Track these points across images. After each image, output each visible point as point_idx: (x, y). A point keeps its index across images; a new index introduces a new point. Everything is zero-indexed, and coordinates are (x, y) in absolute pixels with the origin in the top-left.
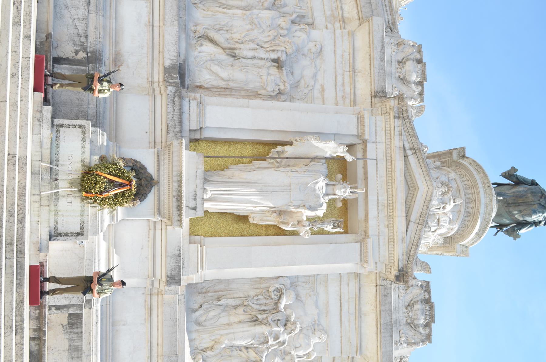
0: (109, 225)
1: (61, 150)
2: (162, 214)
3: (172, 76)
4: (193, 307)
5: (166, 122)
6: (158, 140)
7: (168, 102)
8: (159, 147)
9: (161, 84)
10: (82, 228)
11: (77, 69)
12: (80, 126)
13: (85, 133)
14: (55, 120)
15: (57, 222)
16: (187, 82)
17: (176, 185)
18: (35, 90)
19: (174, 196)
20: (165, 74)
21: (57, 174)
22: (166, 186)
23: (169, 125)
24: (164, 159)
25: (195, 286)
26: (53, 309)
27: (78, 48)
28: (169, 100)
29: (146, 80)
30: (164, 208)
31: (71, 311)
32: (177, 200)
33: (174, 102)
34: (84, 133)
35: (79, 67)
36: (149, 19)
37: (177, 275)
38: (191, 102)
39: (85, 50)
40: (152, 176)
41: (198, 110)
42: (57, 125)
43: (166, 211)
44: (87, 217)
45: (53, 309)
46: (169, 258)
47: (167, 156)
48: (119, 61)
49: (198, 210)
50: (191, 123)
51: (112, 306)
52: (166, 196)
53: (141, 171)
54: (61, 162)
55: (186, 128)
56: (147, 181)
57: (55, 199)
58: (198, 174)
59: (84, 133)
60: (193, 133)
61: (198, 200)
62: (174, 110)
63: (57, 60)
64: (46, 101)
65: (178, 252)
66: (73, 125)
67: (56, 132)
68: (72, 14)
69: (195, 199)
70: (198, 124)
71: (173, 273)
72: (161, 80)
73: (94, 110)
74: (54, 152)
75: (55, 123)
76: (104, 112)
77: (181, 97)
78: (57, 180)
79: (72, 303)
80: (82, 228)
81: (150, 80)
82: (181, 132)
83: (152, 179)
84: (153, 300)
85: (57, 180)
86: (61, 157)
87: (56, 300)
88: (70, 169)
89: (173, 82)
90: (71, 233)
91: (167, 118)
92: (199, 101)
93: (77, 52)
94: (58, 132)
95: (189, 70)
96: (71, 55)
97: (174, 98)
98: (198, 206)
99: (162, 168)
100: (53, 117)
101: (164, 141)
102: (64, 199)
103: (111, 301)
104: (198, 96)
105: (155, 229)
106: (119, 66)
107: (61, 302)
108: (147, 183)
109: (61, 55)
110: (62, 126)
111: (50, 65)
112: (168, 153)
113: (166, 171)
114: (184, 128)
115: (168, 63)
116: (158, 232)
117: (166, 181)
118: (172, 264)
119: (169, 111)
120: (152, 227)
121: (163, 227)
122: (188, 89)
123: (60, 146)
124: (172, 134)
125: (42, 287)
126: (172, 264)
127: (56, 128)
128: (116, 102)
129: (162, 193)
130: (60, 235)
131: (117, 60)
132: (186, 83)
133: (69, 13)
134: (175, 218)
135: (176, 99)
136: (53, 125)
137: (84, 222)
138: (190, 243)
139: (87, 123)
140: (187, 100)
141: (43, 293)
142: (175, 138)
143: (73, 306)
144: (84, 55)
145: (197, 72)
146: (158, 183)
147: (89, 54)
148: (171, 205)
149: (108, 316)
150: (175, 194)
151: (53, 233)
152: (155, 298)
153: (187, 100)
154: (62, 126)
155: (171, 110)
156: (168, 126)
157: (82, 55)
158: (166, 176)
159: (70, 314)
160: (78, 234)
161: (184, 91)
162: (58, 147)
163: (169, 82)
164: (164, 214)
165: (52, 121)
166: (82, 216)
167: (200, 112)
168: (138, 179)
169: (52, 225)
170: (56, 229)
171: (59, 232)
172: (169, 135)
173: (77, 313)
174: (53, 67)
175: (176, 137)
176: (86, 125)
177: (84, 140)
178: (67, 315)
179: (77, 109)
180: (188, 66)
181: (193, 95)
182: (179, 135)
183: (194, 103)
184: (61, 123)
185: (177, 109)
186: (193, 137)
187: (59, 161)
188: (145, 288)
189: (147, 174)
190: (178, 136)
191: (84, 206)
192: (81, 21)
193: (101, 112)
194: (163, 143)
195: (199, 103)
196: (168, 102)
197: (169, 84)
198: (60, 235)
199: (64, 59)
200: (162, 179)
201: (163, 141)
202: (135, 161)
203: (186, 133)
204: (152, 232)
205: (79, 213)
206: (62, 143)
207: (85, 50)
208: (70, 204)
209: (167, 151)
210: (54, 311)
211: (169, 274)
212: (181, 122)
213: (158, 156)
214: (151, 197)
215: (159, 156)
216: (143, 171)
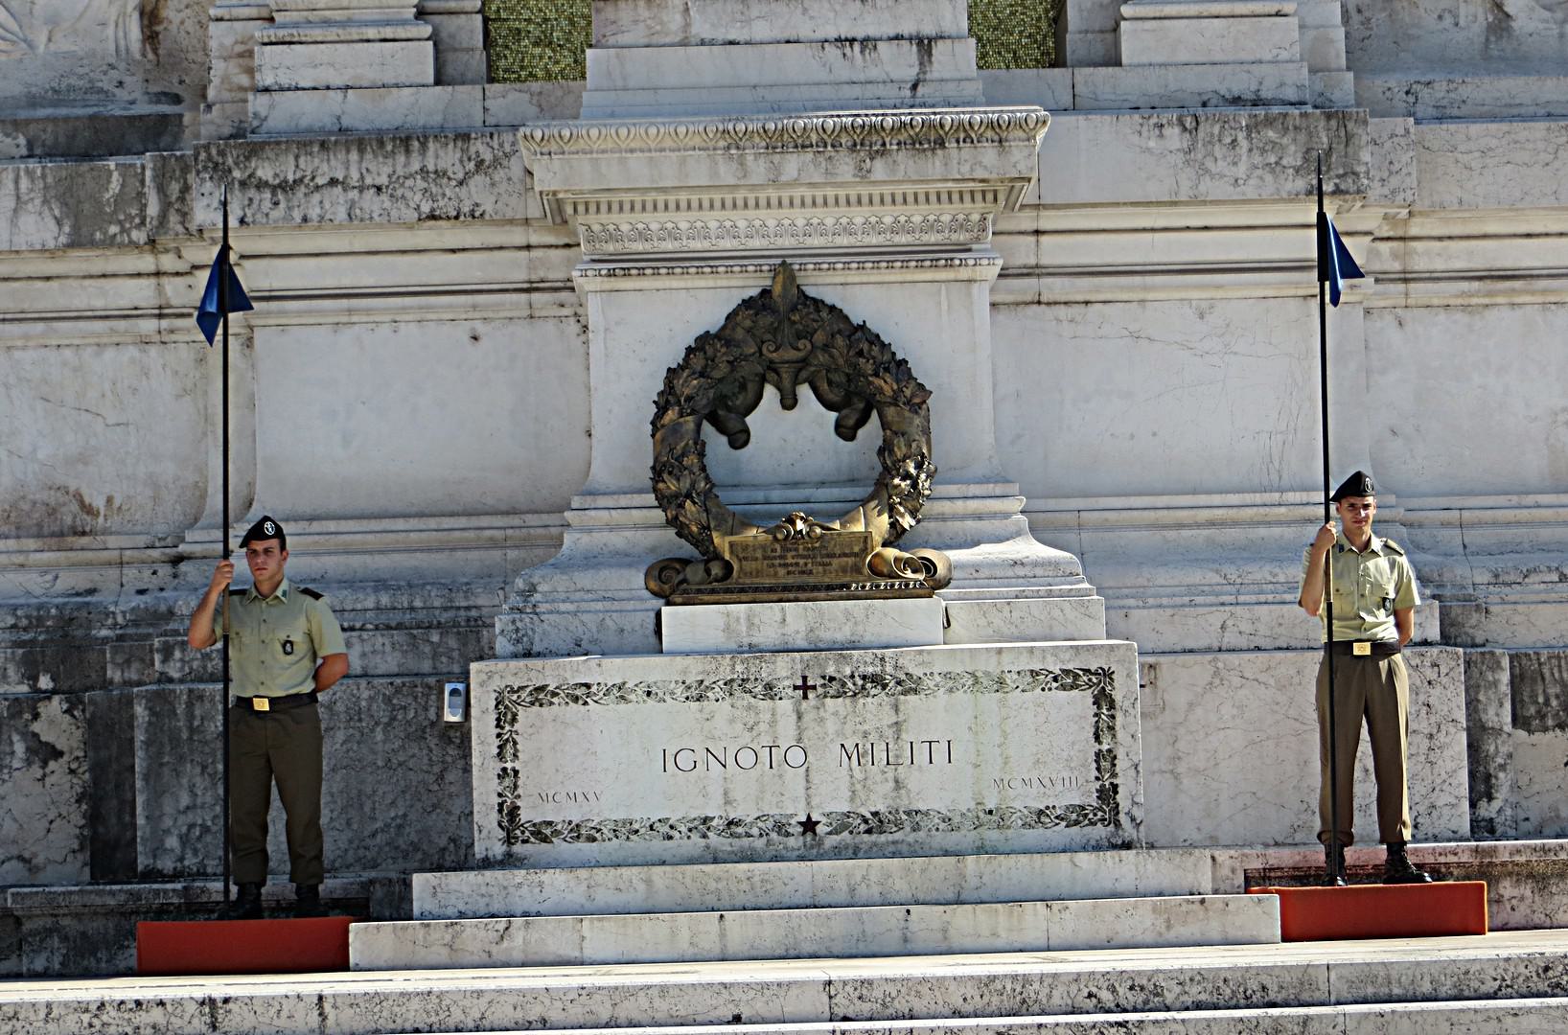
0: (1038, 532)
1: (642, 813)
2: (962, 237)
3: (119, 200)
4: (1478, 29)
5: (410, 227)
6: (514, 268)
7: (288, 217)
8: (553, 265)
9: (168, 262)
10: (1068, 680)
11: (148, 744)
12: (505, 717)
13: (541, 689)
14: (479, 851)
15: (1041, 813)
16: (134, 100)
17: (792, 164)
18: (339, 962)
19: (863, 174)
20: (110, 243)
21: (780, 828)
22: (800, 217)
23: (426, 208)
24: (644, 236)
25: (1356, 18)
26: (1487, 810)
27: (19, 748)
28: (278, 213)
29: (153, 351)
30: (929, 227)
31: (1499, 714)
32: (883, 152)
33: (285, 187)
34: (540, 695)
35: (140, 736)
37: (1302, 137)
38: (269, 81)
39: (28, 706)
40: (747, 303)
41: (317, 34)
42: (509, 840)
43: (947, 213)
44: (1006, 658)
45: (1487, 810)
46: (1207, 187)
47: (624, 222)
48: (52, 512)
49: (928, 29)
50: (395, 74)
51: (1471, 493)
52: (859, 216)
54: (714, 810)
55: (431, 104)
56: (774, 331)
57: (916, 828)
58: (721, 35)
59: (540, 695)
60: (454, 64)
61: (872, 31)
62: (333, 182)
63: (107, 851)
64: (398, 907)
65: (1173, 132)
66: (501, 756)
67: (545, 839)
69: (867, 43)
70: (401, 33)
71: (1293, 157)
72: (147, 262)
73: (380, 640)
74: (658, 846)
75: (498, 849)
76: (380, 584)
77: (247, 140)
78: (809, 826)
79: (1461, 716)
80: (1068, 680)
81: (149, 326)
82: (464, 137)
83: (758, 305)
84: (1439, 265)
85: (809, 826)
86: (680, 810)
87: (1442, 800)
88: (747, 759)
89: (161, 190)
90: (1097, 738)
91: (390, 223)
92: (259, 31)
93: (44, 753)
94: (541, 833)
95: (57, 96)
96: (62, 781)
97: (261, 185)
98: (907, 29)
99: (697, 245)
100: (458, 858)
101: (518, 237)
102: (913, 780)
103: (1444, 502)
104: (220, 37)
106: (89, 510)
107: (1452, 774)
109: (66, 834)
110: (510, 815)
111: (157, 892)
112: (604, 217)
113: (712, 220)
114: (437, 120)
115: (40, 227)
116: (1054, 251)
117: (770, 218)
118: (1241, 170)
119: (341, 214)
120: (1027, 287)
121: (1026, 221)
122: (177, 99)
123: (621, 815)
124: (478, 191)
125: (1376, 873)
126: (1241, 170)
127: (523, 838)
128: (312, 518)
129: (844, 240)
130: (1108, 794)
131: (63, 523)
132: (144, 108)
134: (987, 160)
135: (265, 172)
136: (509, 862)
137: (1034, 673)
138: (1116, 62)
139: (486, 680)
140: (258, 104)
141: (1397, 866)
142: (499, 175)
143: (1472, 705)
144: (56, 706)
145: (64, 45)
146: (784, 269)
147: (45, 682)
148: (910, 189)
149: (1523, 514)
150: (845, 166)
151: (1100, 832)
152: (1426, 257)
153: (258, 104)
154: (510, 815)
155: (336, 202)
156: (432, 217)
157: (55, 723)
158: (740, 219)
159: (1517, 721)
160: (1103, 699)
161: (205, 125)
162: (626, 829)
163: (163, 217)
164: (958, 226)
165: (487, 864)
166: (1001, 682)
167: (327, 23)
168: (763, 380)
169: (1061, 833)
170: (1078, 816)
171: (1093, 800)
172: (488, 206)
173: (1512, 682)
174: (152, 875)
175: (496, 163)
176: (498, 683)
177: (581, 694)
178: (1522, 734)
179: (379, 735)
180: (33, 102)
181: (219, 68)
182: (478, 147)
183: (275, 64)
184: (494, 816)
185: (327, 167)
186: (478, 61)
187: (706, 820)
188: (1368, 312)
190: (488, 156)
191: (947, 675)
193: (385, 600)
194: (534, 240)
195: (273, 34)
196: (288, 217)
197: (173, 218)
198: (1108, 794)
199: (94, 818)
200: (757, 243)
201: (521, 241)
202: (662, 408)
203: (466, 101)
204: (1055, 288)
205: (990, 699)
206: (606, 810)
207: (28, 706)
208: (940, 752)
209: (595, 221)
210: (1496, 804)
211: (1301, 184)
212: (406, 139)
213: (627, 273)
214: (868, 300)
215: (623, 265)
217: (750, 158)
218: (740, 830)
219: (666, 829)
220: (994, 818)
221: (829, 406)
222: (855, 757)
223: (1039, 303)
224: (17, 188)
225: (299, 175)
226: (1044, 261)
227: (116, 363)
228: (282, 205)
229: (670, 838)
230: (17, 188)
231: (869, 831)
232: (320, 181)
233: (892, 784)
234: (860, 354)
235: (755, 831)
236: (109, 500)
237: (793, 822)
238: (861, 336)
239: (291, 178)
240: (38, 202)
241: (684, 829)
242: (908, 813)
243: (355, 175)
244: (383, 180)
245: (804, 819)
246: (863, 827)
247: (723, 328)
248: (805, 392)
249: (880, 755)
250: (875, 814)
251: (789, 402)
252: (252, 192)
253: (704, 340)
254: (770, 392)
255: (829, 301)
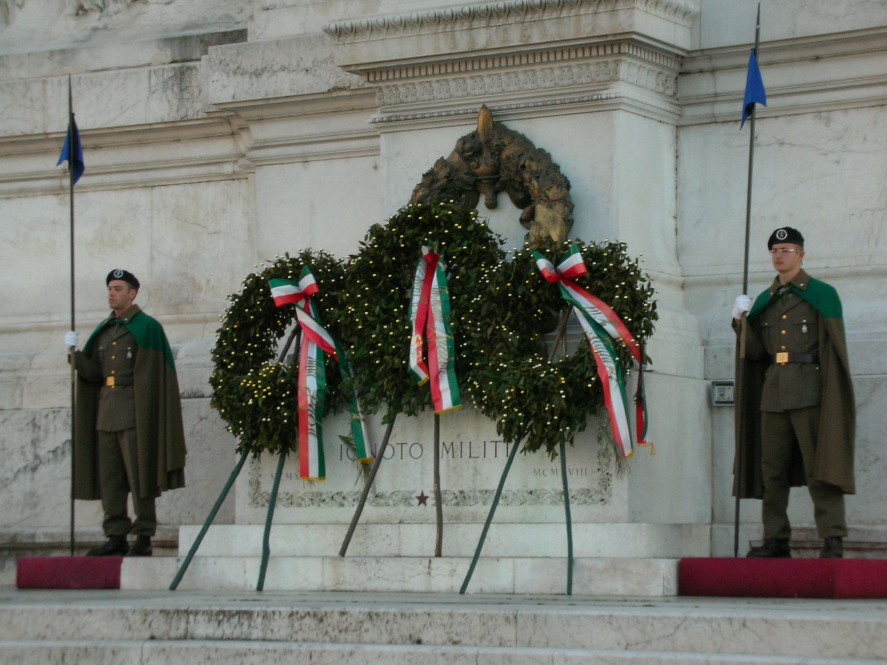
23: (332, 83)
36: (46, 192)
53: (443, 182)
68: (22, 465)
105: (715, 98)
106: (197, 288)
108: (486, 154)
120: (704, 111)
133: (21, 477)
151: (598, 508)
189: (457, 158)
192: (42, 433)
216: (443, 174)
217: (458, 34)
218: (382, 501)
219: (339, 499)
220: (533, 497)
221: (520, 204)
222: (451, 452)
223: (716, 122)
224: (150, 83)
225: (264, 65)
226: (720, 90)
227: (210, 193)
228: (255, 85)
229: (343, 505)
230: (150, 83)
231: (457, 504)
232: (276, 68)
233: (471, 471)
234: (523, 167)
235: (391, 502)
236: (208, 281)
237: (414, 496)
238: (542, 155)
239: (260, 68)
240: (160, 91)
241: (350, 499)
242: (481, 492)
243: (294, 63)
244: (309, 65)
245: (419, 494)
246: (454, 501)
247: (452, 154)
248: (505, 200)
249: (466, 451)
250: (461, 492)
251: (493, 205)
252: (239, 78)
253: (442, 162)
254: (482, 199)
255: (521, 131)
